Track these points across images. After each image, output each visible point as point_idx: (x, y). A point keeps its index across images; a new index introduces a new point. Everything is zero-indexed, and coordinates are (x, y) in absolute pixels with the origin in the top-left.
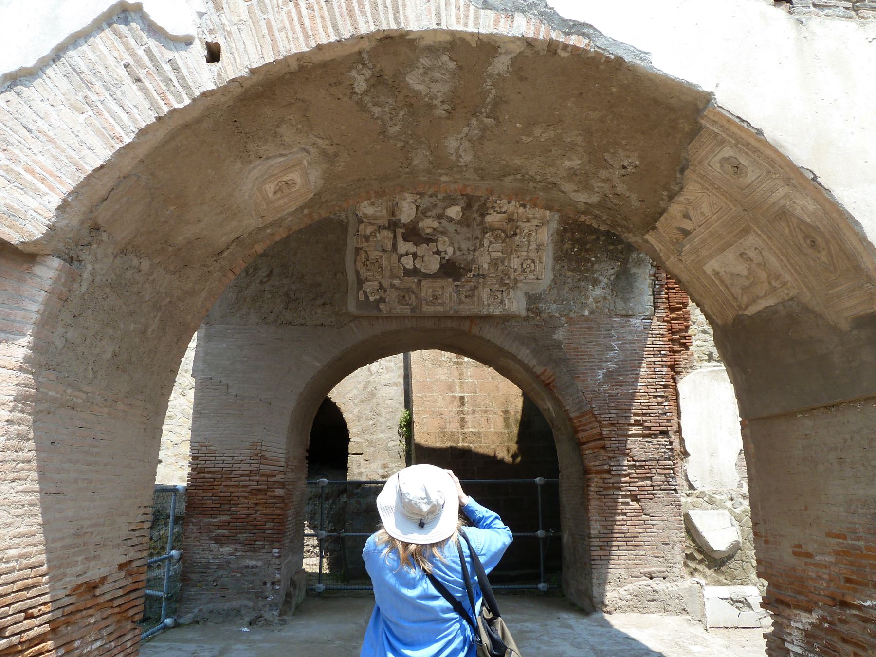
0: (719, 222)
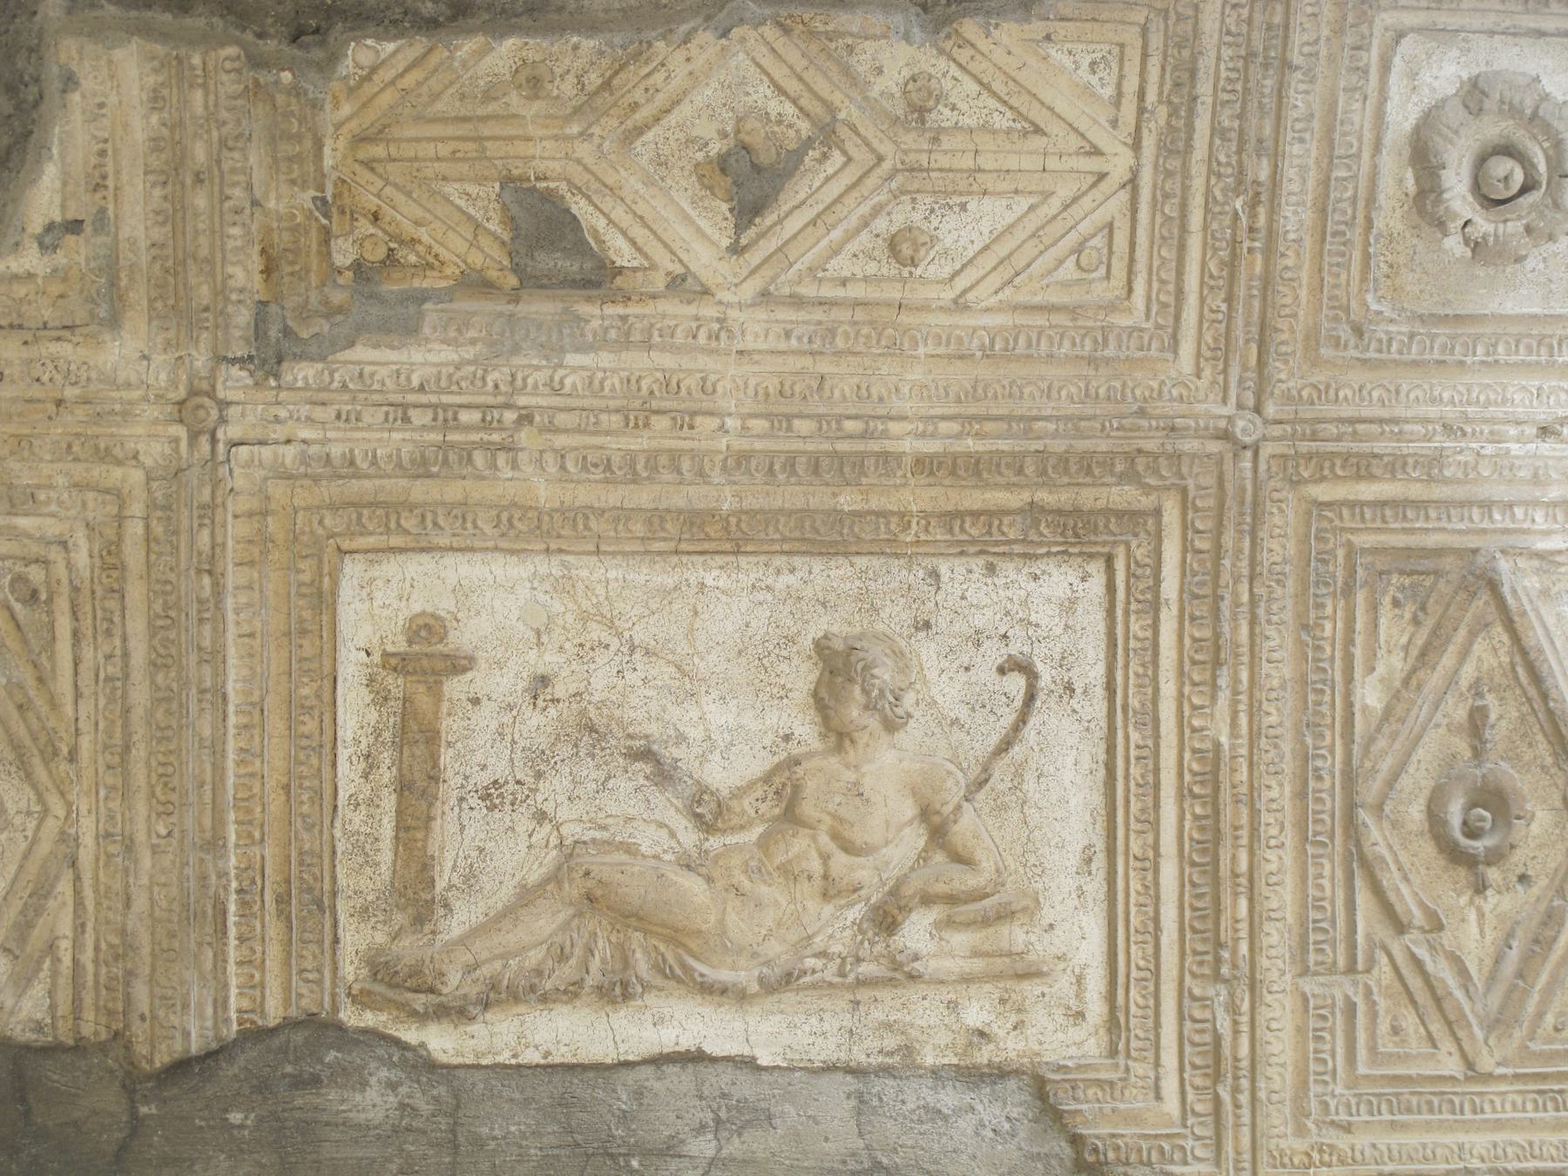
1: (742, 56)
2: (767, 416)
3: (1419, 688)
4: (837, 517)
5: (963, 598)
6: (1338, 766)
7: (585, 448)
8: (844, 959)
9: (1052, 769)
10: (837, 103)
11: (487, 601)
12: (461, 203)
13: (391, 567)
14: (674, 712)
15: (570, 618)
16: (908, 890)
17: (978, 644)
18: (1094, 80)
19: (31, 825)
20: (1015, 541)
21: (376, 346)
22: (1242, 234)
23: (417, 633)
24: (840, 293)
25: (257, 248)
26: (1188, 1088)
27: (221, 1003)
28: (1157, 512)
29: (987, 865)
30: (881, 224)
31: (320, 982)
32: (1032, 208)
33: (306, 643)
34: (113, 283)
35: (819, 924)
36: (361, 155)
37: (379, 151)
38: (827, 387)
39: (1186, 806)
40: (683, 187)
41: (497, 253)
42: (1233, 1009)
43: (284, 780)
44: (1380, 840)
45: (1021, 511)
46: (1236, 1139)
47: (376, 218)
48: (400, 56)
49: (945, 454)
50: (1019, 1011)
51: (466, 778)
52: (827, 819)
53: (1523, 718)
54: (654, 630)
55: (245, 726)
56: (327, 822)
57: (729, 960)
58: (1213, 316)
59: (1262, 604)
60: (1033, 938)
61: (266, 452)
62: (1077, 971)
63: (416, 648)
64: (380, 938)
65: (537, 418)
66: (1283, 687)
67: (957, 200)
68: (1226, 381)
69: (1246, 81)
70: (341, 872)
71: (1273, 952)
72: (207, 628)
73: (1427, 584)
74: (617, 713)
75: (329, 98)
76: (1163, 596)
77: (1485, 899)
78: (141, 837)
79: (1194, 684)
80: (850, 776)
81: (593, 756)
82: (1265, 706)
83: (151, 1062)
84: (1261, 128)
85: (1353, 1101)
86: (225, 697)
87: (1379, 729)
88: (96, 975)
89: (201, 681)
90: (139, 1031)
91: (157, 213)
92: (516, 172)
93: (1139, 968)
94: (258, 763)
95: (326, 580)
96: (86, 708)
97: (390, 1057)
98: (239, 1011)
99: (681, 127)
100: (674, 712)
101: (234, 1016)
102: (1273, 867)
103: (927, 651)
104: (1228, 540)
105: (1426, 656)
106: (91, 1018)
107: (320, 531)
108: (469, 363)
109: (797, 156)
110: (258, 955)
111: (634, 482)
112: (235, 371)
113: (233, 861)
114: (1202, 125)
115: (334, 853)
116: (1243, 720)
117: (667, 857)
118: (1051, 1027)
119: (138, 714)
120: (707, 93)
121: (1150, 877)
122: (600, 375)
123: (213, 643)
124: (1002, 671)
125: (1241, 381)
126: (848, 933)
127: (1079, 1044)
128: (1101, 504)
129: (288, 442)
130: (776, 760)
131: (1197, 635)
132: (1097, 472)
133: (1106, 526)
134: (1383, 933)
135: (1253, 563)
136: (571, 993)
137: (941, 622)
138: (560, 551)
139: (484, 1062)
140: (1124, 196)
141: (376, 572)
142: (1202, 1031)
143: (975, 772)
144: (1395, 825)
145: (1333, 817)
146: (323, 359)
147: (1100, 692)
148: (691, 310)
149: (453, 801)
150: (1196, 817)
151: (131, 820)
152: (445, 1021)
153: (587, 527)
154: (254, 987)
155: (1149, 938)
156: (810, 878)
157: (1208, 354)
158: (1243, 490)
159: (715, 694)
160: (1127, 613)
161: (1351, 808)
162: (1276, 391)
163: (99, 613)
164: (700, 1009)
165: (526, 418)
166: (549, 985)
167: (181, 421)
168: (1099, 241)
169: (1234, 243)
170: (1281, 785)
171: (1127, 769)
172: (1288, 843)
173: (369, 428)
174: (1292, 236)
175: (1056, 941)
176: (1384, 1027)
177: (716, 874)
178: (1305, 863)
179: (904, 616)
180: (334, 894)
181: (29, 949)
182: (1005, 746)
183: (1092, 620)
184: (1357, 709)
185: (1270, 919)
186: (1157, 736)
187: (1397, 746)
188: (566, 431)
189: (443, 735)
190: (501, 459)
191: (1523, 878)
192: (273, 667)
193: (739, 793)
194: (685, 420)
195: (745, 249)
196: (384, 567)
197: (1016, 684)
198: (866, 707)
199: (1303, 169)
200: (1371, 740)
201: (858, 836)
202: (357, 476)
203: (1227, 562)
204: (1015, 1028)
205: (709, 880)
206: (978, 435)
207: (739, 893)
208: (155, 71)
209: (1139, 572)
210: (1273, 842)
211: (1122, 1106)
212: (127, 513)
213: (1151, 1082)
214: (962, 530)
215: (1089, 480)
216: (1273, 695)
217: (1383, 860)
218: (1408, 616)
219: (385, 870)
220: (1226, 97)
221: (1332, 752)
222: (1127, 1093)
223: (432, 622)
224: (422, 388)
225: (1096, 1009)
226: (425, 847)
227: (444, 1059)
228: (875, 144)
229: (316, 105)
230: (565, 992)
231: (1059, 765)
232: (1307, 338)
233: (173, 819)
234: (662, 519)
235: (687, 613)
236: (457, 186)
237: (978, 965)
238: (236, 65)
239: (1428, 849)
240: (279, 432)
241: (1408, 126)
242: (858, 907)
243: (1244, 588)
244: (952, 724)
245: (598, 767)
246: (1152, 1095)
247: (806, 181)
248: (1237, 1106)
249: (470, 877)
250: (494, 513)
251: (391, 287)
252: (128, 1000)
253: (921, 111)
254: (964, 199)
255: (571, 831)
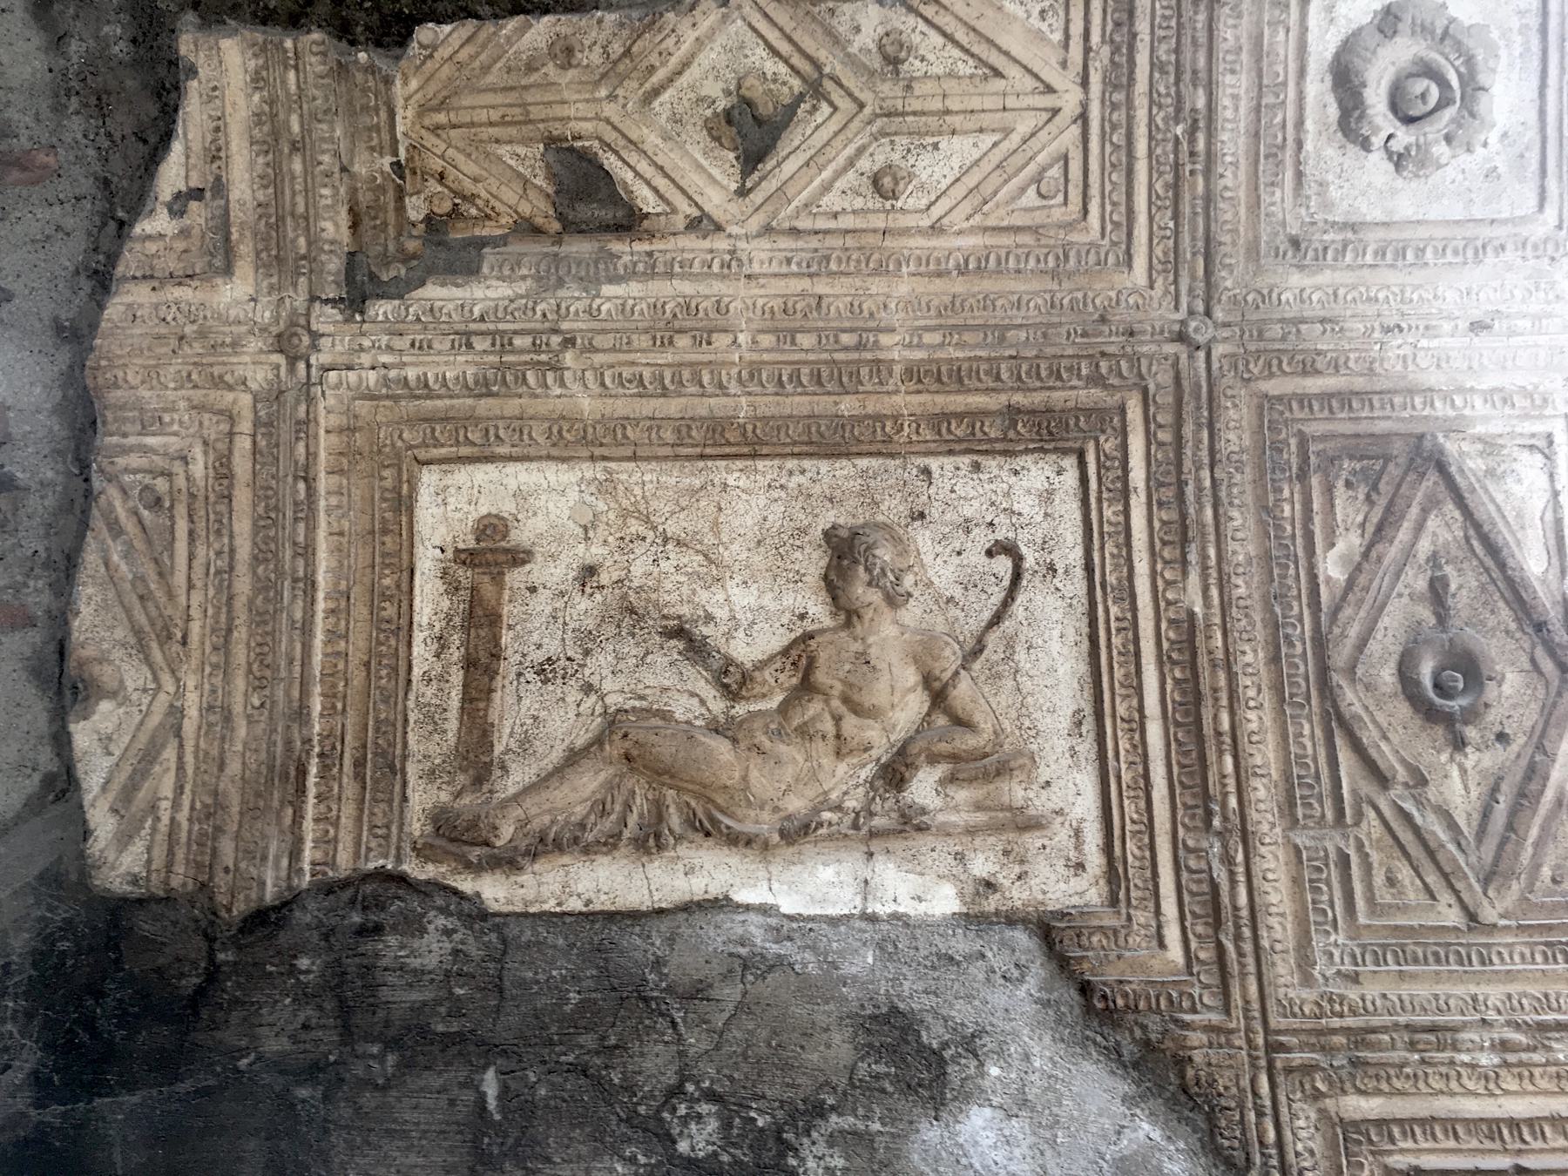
0: (959, 286)
1: (739, 22)
2: (775, 331)
3: (1379, 560)
4: (840, 423)
5: (953, 491)
6: (1308, 635)
7: (621, 364)
8: (857, 814)
9: (1040, 642)
10: (822, 59)
11: (542, 503)
12: (512, 163)
13: (462, 476)
14: (703, 596)
15: (612, 515)
16: (914, 749)
17: (968, 531)
18: (1044, 27)
19: (146, 700)
20: (997, 440)
21: (442, 285)
22: (1184, 156)
23: (484, 531)
24: (832, 225)
25: (346, 207)
26: (1191, 936)
27: (295, 854)
28: (1122, 410)
29: (987, 727)
30: (864, 164)
31: (387, 837)
32: (995, 145)
33: (388, 539)
34: (227, 239)
35: (834, 780)
36: (427, 122)
37: (441, 118)
38: (824, 305)
39: (1166, 670)
40: (696, 143)
41: (543, 205)
42: (1228, 860)
43: (366, 658)
44: (1355, 701)
45: (999, 413)
46: (1244, 988)
47: (442, 177)
48: (455, 35)
49: (930, 361)
50: (1022, 862)
51: (524, 655)
52: (839, 686)
53: (1483, 588)
54: (685, 524)
55: (333, 611)
56: (401, 694)
57: (753, 814)
58: (1162, 233)
59: (1224, 488)
60: (1031, 794)
61: (352, 376)
62: (1074, 824)
63: (483, 544)
64: (444, 797)
65: (579, 341)
66: (1249, 561)
67: (929, 140)
68: (1177, 290)
69: (1180, 16)
70: (412, 738)
71: (1262, 806)
72: (302, 525)
73: (1377, 468)
74: (654, 596)
75: (399, 76)
76: (1131, 485)
77: (1466, 756)
78: (238, 708)
79: (1166, 562)
80: (857, 646)
81: (633, 635)
82: (1234, 580)
83: (229, 910)
84: (1194, 61)
85: (1358, 951)
86: (313, 583)
87: (1344, 598)
88: (190, 832)
89: (294, 570)
90: (222, 881)
91: (262, 178)
92: (555, 133)
93: (1133, 822)
94: (343, 644)
95: (405, 486)
96: (197, 598)
97: (448, 906)
98: (313, 863)
99: (692, 87)
100: (703, 596)
101: (307, 867)
102: (1254, 726)
103: (922, 539)
104: (1188, 430)
105: (1381, 532)
106: (181, 871)
107: (399, 444)
108: (522, 297)
109: (792, 109)
110: (334, 813)
111: (664, 395)
112: (328, 310)
113: (317, 728)
114: (1142, 59)
115: (406, 721)
116: (1214, 592)
117: (698, 723)
118: (1053, 877)
119: (240, 603)
120: (711, 56)
121: (1137, 736)
122: (631, 302)
123: (306, 537)
124: (989, 553)
125: (1191, 290)
126: (861, 790)
127: (1081, 894)
128: (1071, 404)
129: (373, 368)
130: (793, 636)
131: (1165, 518)
132: (1065, 376)
133: (1077, 424)
134: (1368, 788)
135: (1212, 451)
136: (610, 844)
137: (934, 512)
138: (604, 458)
139: (532, 910)
140: (1075, 130)
141: (448, 480)
142: (1199, 882)
143: (970, 643)
144: (1368, 687)
145: (1307, 680)
146: (401, 297)
147: (1079, 572)
148: (706, 244)
149: (512, 676)
150: (1177, 681)
151: (229, 693)
152: (498, 872)
153: (625, 436)
154: (327, 842)
155: (1141, 794)
156: (824, 737)
157: (1160, 267)
158: (1200, 387)
159: (738, 579)
160: (1099, 500)
161: (1324, 671)
162: (1224, 298)
163: (212, 516)
164: (727, 860)
165: (569, 342)
166: (590, 837)
167: (281, 351)
168: (1055, 172)
169: (1177, 166)
170: (1255, 651)
171: (1109, 640)
172: (1266, 705)
173: (439, 353)
174: (1228, 159)
175: (1054, 798)
176: (1379, 879)
177: (740, 736)
178: (1285, 722)
179: (901, 508)
180: (405, 758)
181: (134, 809)
182: (997, 619)
183: (1069, 509)
184: (1321, 579)
185: (1255, 774)
186: (1134, 609)
187: (1362, 614)
188: (604, 351)
189: (505, 618)
190: (550, 376)
191: (1502, 737)
192: (360, 560)
193: (761, 665)
194: (704, 337)
195: (750, 190)
196: (457, 476)
197: (1003, 565)
198: (869, 584)
199: (1235, 97)
200: (1336, 611)
201: (867, 700)
202: (430, 396)
203: (1188, 452)
204: (1019, 878)
205: (735, 741)
206: (961, 345)
207: (760, 751)
208: (255, 55)
209: (1108, 464)
210: (1252, 704)
211: (1128, 954)
212: (236, 430)
213: (1153, 930)
214: (949, 431)
215: (1059, 384)
216: (1241, 570)
217: (1360, 719)
218: (1361, 497)
219: (451, 736)
220: (1162, 33)
221: (1301, 620)
222: (1130, 940)
223: (495, 521)
224: (482, 319)
225: (1095, 860)
226: (486, 716)
227: (494, 907)
228: (857, 93)
229: (388, 81)
230: (605, 844)
231: (1046, 637)
232: (1248, 251)
233: (267, 692)
234: (689, 427)
235: (712, 509)
236: (508, 148)
237: (981, 817)
238: (321, 48)
239: (1404, 709)
240: (366, 359)
241: (1329, 55)
242: (870, 766)
243: (1205, 474)
244: (948, 601)
245: (638, 644)
246: (1154, 943)
247: (799, 130)
248: (1241, 954)
249: (526, 743)
250: (546, 425)
251: (457, 234)
252: (215, 852)
253: (894, 62)
254: (936, 139)
255: (614, 700)
